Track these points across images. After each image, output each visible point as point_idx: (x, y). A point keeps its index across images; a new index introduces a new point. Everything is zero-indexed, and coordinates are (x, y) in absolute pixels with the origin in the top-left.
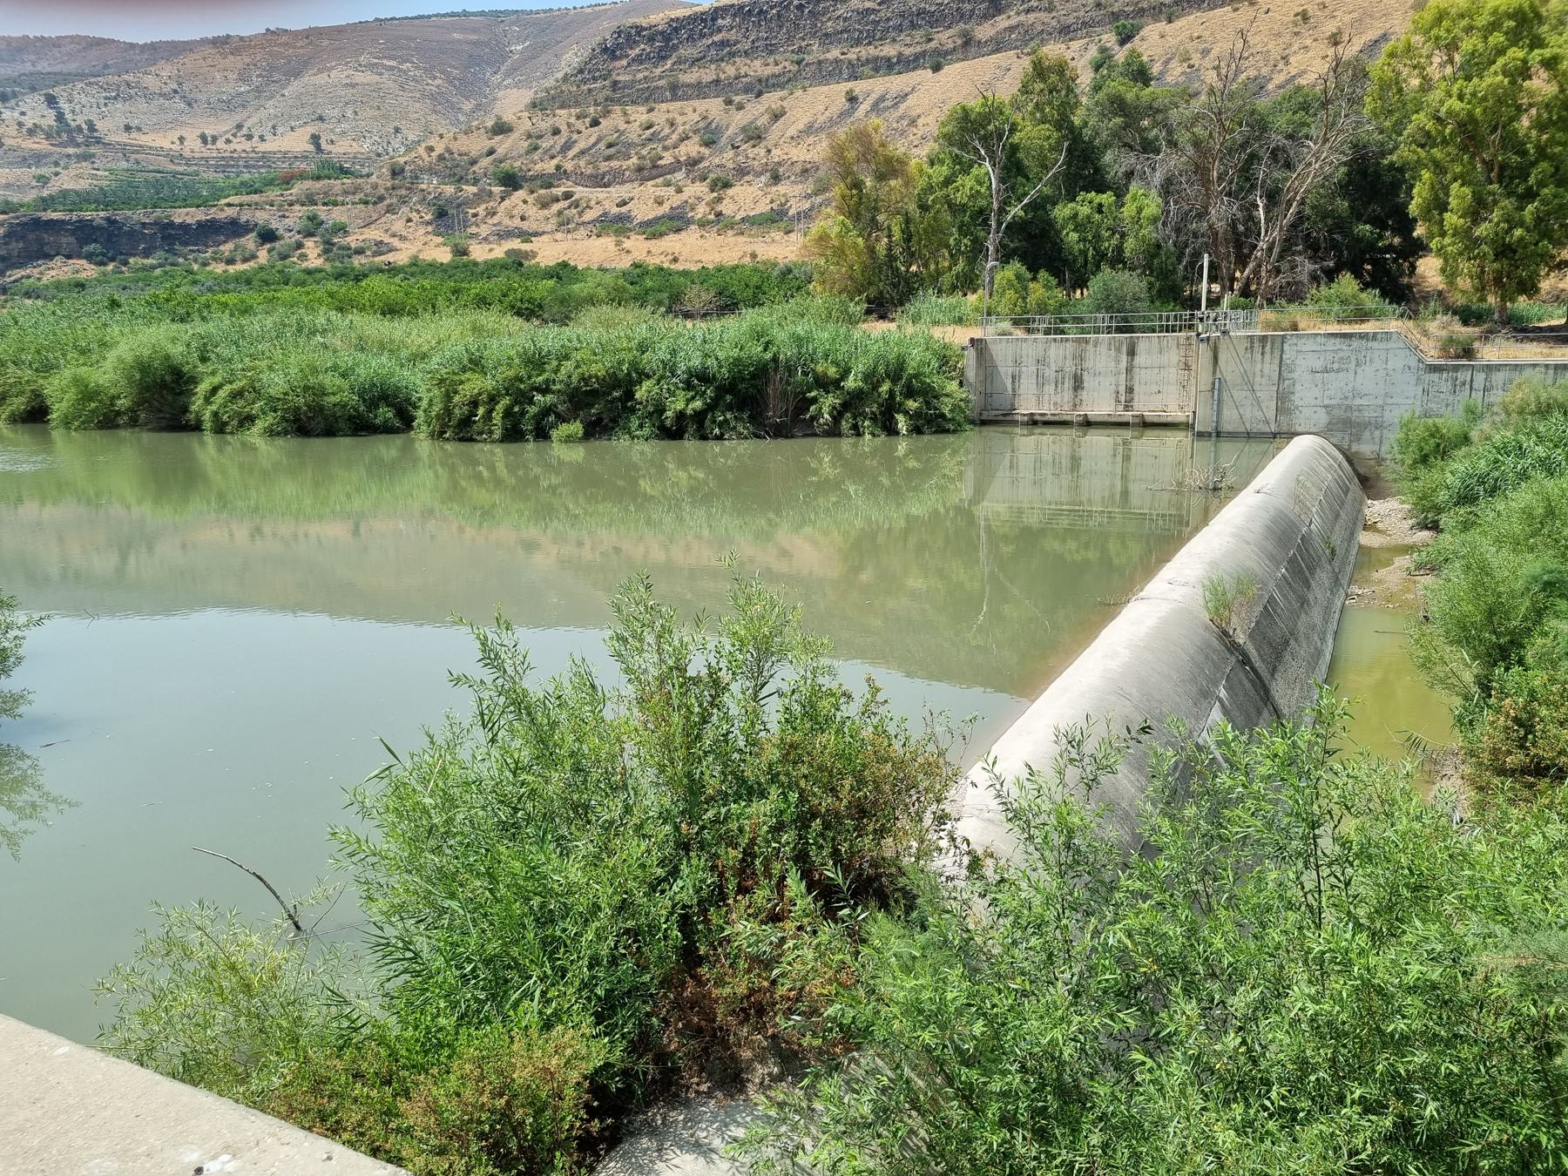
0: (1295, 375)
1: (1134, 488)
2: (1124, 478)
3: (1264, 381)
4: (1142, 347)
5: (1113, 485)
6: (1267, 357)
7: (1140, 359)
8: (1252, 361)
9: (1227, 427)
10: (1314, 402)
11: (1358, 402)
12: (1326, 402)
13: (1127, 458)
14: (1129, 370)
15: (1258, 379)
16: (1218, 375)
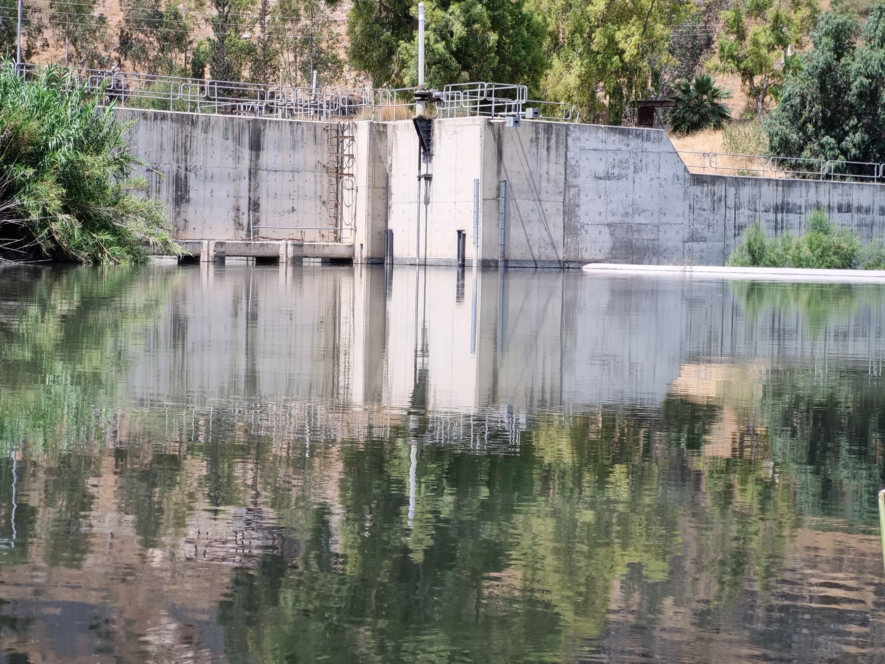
0: (579, 181)
1: (265, 367)
2: (251, 350)
3: (550, 187)
4: (269, 137)
5: (234, 365)
6: (553, 152)
7: (268, 157)
8: (538, 159)
9: (516, 253)
10: (599, 219)
11: (637, 219)
12: (610, 219)
13: (253, 317)
14: (253, 173)
15: (544, 184)
16: (503, 178)
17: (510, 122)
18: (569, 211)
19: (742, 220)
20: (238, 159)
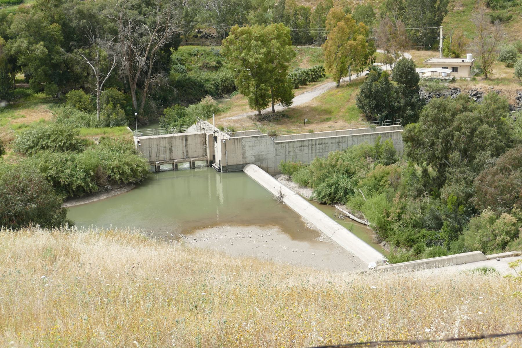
6: (238, 144)
14: (186, 145)
19: (290, 150)
20: (183, 143)
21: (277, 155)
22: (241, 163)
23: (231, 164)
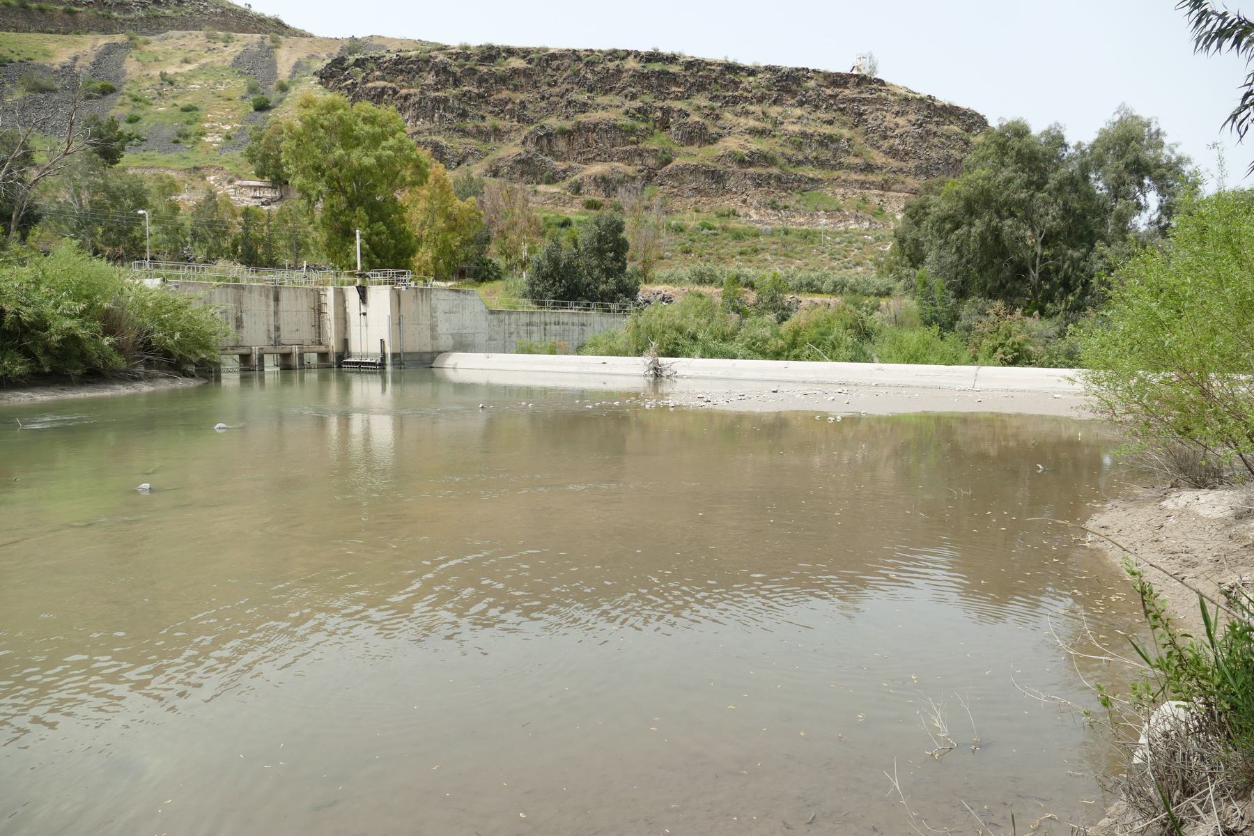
7: (284, 303)
14: (276, 313)
17: (404, 288)
18: (433, 328)
20: (268, 306)
21: (490, 339)
22: (429, 349)
23: (409, 350)
